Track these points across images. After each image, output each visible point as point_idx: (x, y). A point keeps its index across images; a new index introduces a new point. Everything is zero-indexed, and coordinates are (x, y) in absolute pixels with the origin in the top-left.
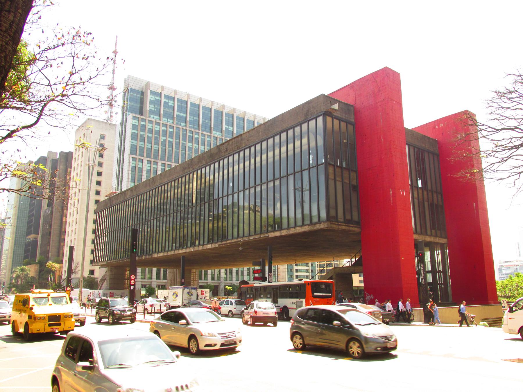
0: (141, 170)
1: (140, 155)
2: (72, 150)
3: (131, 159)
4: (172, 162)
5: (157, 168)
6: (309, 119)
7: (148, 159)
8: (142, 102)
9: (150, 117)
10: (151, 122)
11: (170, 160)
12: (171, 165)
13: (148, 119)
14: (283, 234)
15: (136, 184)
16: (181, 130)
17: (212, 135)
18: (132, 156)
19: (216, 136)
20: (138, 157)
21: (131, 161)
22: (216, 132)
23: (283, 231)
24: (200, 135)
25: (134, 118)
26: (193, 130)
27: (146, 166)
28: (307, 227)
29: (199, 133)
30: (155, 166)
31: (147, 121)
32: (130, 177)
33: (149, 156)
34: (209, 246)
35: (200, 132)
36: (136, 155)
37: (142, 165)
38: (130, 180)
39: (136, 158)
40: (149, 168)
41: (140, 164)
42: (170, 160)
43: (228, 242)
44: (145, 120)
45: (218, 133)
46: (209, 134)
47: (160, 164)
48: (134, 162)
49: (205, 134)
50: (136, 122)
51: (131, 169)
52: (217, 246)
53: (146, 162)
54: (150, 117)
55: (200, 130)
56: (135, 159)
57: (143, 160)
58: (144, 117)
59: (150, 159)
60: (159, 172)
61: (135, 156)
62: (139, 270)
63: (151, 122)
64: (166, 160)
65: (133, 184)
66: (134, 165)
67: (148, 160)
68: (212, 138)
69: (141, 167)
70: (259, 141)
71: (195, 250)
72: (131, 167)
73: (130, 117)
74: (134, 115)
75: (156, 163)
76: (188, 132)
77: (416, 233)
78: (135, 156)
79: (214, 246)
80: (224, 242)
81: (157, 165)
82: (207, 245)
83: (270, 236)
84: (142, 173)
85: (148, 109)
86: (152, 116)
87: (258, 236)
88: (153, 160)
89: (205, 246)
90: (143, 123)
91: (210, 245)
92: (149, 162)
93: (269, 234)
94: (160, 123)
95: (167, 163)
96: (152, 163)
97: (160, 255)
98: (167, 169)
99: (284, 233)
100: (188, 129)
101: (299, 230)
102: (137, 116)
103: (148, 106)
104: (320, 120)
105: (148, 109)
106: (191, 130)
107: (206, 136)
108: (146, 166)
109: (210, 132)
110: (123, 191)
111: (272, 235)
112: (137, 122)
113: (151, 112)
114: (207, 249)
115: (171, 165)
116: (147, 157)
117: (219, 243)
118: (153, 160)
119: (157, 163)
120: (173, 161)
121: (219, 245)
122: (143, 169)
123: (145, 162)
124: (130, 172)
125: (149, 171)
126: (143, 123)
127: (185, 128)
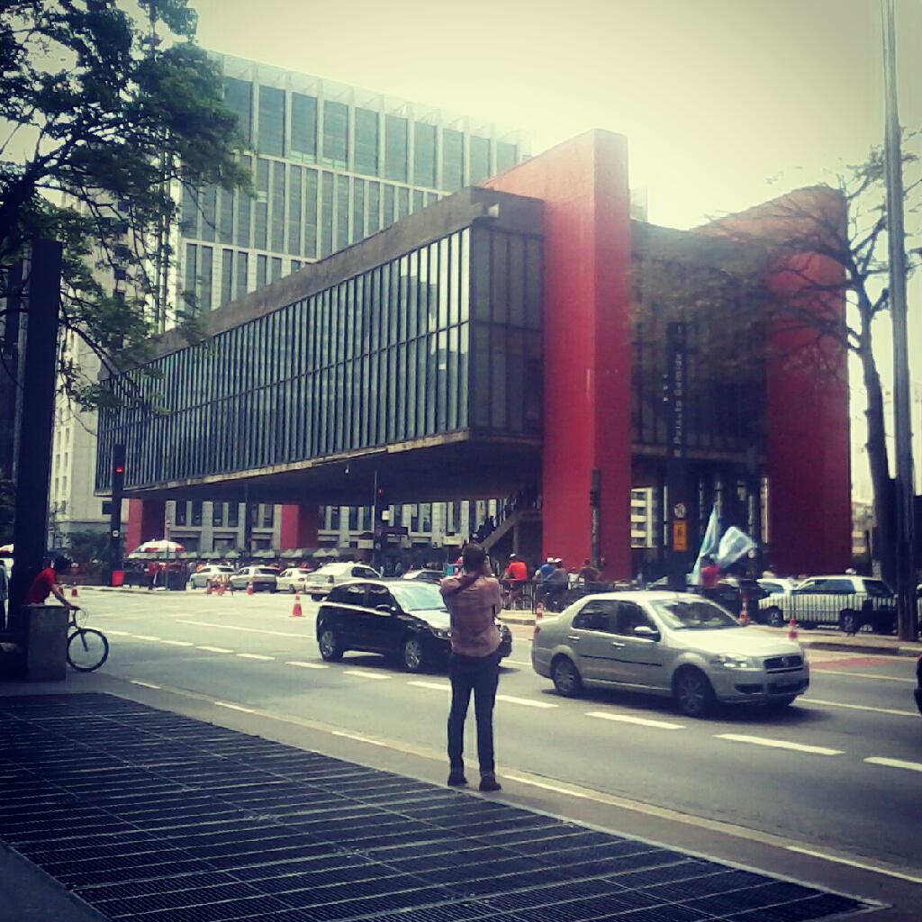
11: (311, 250)
14: (408, 448)
28: (440, 437)
52: (310, 466)
57: (247, 254)
64: (302, 250)
67: (259, 255)
79: (308, 464)
82: (294, 462)
83: (390, 451)
91: (300, 463)
93: (389, 447)
99: (409, 446)
101: (430, 442)
111: (392, 449)
116: (256, 247)
117: (313, 461)
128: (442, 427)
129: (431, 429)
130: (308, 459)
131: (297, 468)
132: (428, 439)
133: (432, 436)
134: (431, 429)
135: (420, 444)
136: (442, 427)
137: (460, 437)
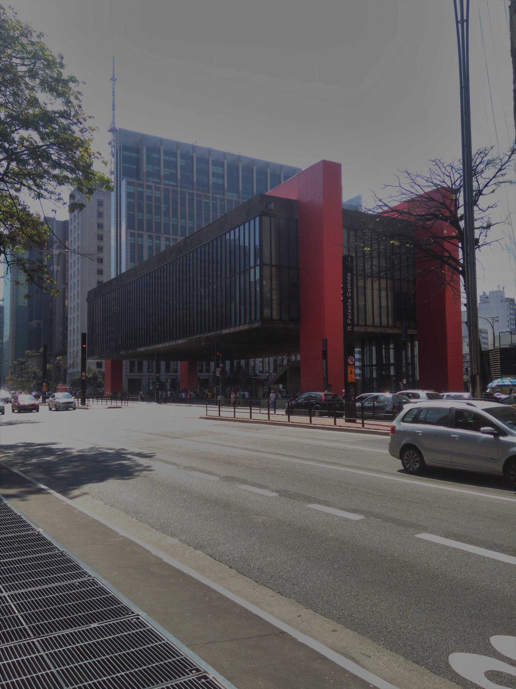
0: (141, 247)
1: (138, 230)
2: (68, 219)
3: (129, 234)
4: (178, 236)
5: (160, 244)
6: (249, 219)
7: (149, 233)
8: (138, 161)
9: (148, 181)
10: (149, 187)
12: (177, 239)
13: (145, 183)
14: (231, 331)
15: (137, 264)
16: (187, 194)
17: (226, 198)
18: (129, 231)
19: (231, 198)
20: (136, 232)
21: (129, 237)
22: (230, 194)
23: (231, 329)
24: (211, 198)
25: (129, 184)
26: (201, 193)
27: (146, 242)
28: (247, 325)
29: (209, 196)
30: (158, 242)
31: (145, 187)
32: (129, 257)
33: (149, 229)
34: (180, 342)
35: (211, 195)
36: (134, 229)
37: (143, 241)
38: (129, 260)
39: (135, 233)
40: (151, 244)
41: (140, 239)
42: (175, 233)
43: (194, 337)
44: (142, 186)
45: (234, 194)
46: (221, 197)
47: (163, 239)
48: (133, 238)
49: (217, 198)
50: (132, 189)
51: (129, 247)
52: (186, 341)
53: (147, 237)
54: (148, 181)
55: (211, 192)
56: (132, 235)
57: (142, 235)
58: (140, 182)
59: (151, 234)
60: (163, 249)
61: (133, 231)
62: (145, 363)
63: (149, 187)
65: (133, 264)
66: (133, 242)
67: (148, 235)
68: (226, 201)
69: (140, 243)
70: (215, 238)
71: (170, 345)
72: (129, 244)
73: (124, 183)
74: (129, 180)
75: (159, 238)
76: (195, 196)
77: (373, 326)
78: (133, 231)
80: (191, 338)
81: (160, 240)
82: (178, 340)
84: (143, 250)
85: (145, 171)
86: (150, 179)
87: (213, 333)
88: (154, 234)
89: (177, 341)
90: (140, 189)
91: (181, 340)
92: (150, 237)
93: (222, 331)
94: (160, 188)
95: (172, 237)
96: (154, 238)
97: (143, 349)
98: (172, 244)
99: (232, 330)
100: (195, 192)
102: (131, 181)
103: (145, 167)
104: (257, 219)
105: (145, 171)
106: (199, 193)
107: (218, 201)
108: (146, 242)
109: (224, 195)
110: (122, 272)
112: (132, 188)
113: (149, 174)
114: (178, 344)
115: (177, 239)
116: (147, 231)
117: (187, 339)
118: (154, 234)
119: (160, 237)
120: (179, 233)
121: (187, 340)
122: (144, 246)
123: (145, 237)
124: (129, 250)
125: (150, 248)
126: (140, 189)
127: (191, 191)
128: (248, 320)
129: (243, 322)
130: (185, 339)
131: (179, 343)
132: (241, 326)
133: (243, 324)
134: (243, 322)
135: (237, 329)
136: (248, 320)
137: (257, 325)
